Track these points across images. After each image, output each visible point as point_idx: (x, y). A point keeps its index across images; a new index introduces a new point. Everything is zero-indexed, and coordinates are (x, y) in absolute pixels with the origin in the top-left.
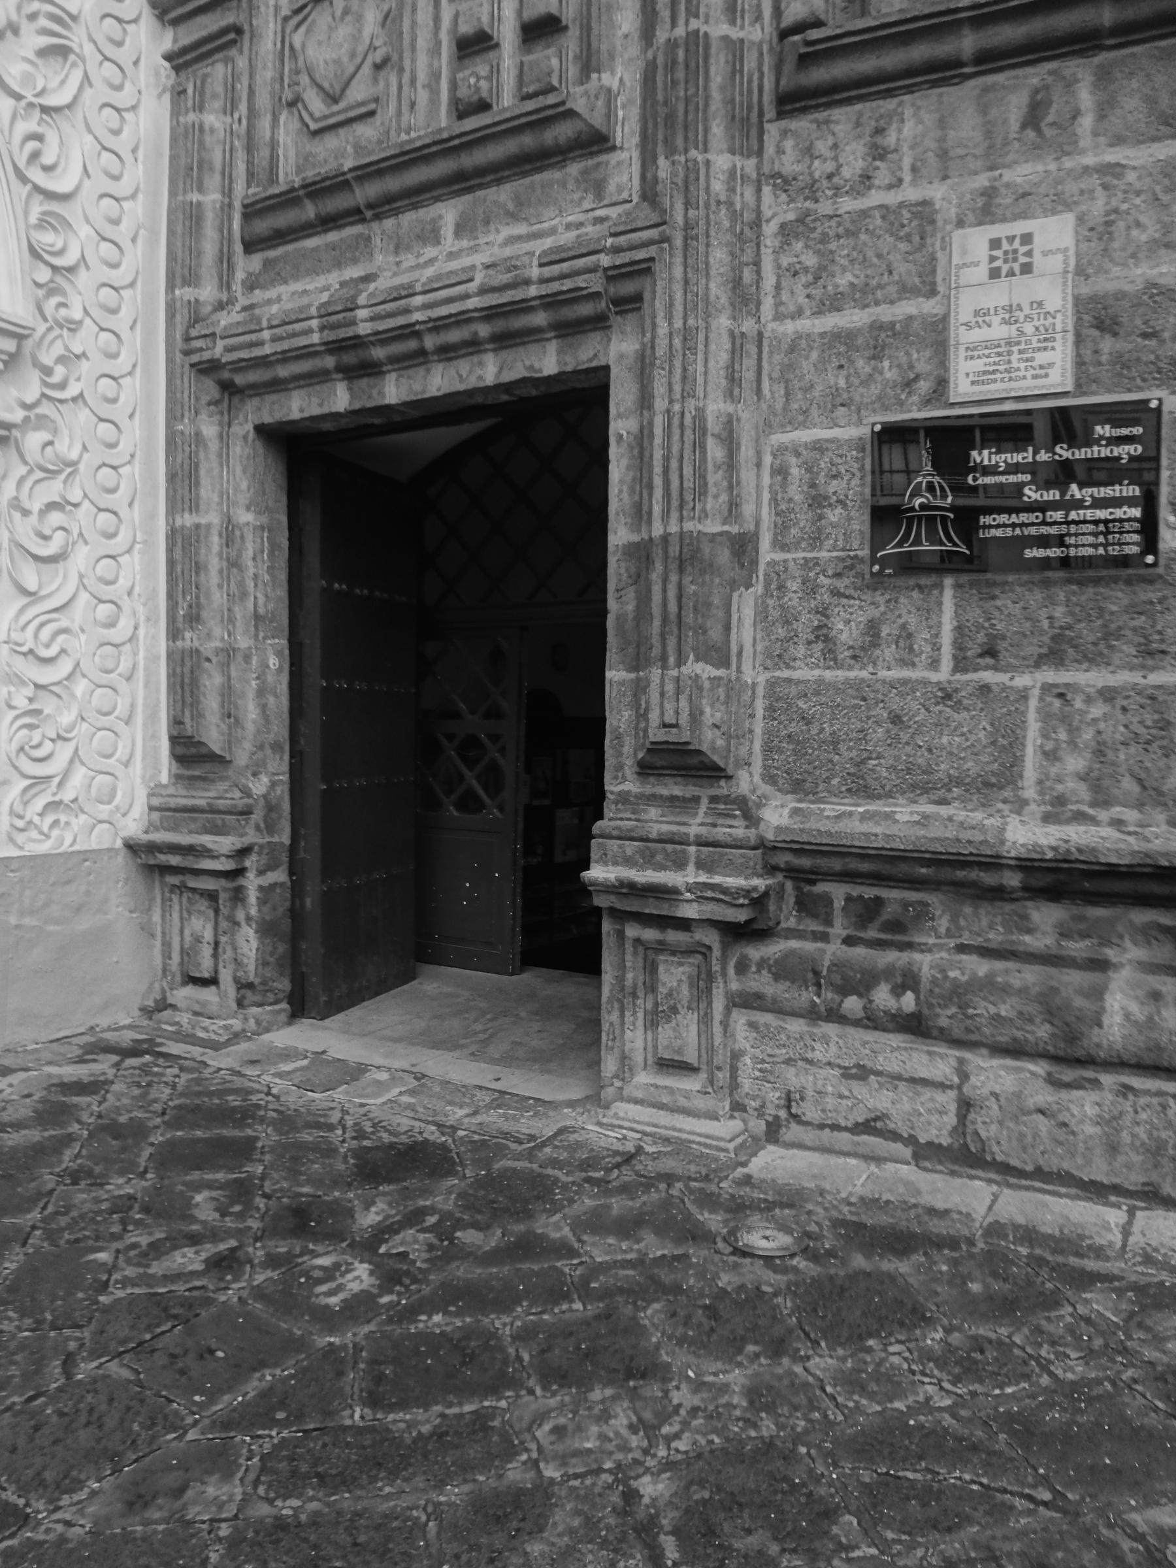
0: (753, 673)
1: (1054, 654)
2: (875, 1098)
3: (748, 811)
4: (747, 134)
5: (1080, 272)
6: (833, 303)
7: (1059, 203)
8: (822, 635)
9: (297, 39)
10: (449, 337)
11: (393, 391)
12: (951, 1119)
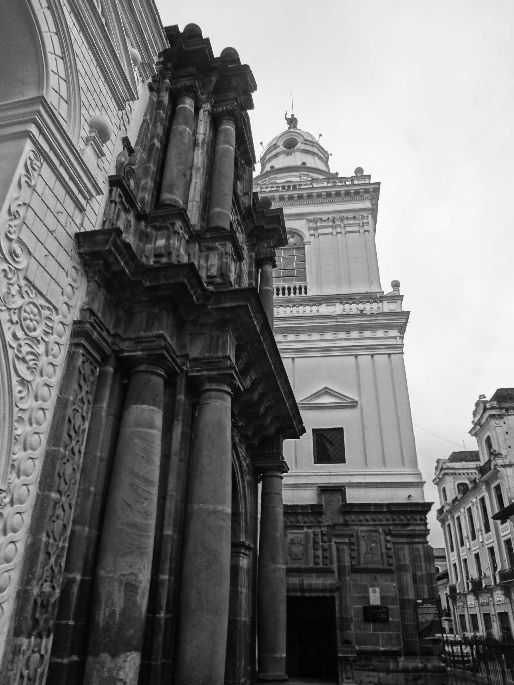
0: (354, 632)
1: (381, 630)
2: (370, 679)
3: (354, 647)
4: (349, 576)
5: (381, 593)
6: (358, 593)
7: (377, 586)
8: (360, 628)
9: (290, 547)
10: (317, 590)
11: (307, 595)
12: (378, 680)
